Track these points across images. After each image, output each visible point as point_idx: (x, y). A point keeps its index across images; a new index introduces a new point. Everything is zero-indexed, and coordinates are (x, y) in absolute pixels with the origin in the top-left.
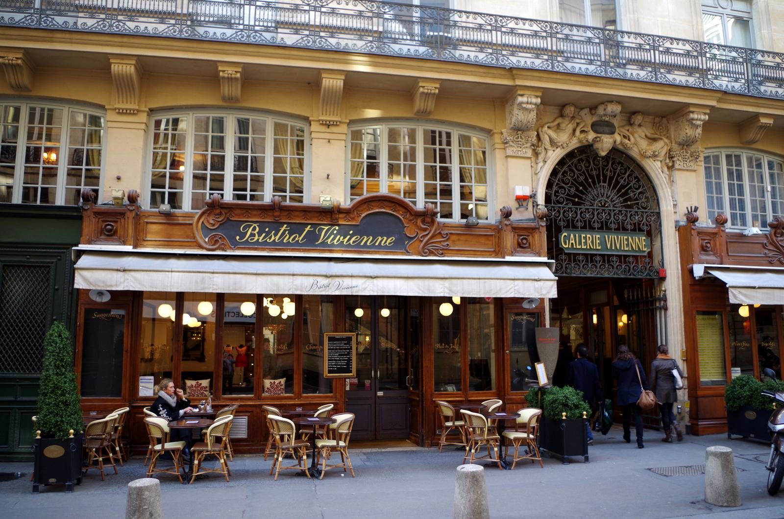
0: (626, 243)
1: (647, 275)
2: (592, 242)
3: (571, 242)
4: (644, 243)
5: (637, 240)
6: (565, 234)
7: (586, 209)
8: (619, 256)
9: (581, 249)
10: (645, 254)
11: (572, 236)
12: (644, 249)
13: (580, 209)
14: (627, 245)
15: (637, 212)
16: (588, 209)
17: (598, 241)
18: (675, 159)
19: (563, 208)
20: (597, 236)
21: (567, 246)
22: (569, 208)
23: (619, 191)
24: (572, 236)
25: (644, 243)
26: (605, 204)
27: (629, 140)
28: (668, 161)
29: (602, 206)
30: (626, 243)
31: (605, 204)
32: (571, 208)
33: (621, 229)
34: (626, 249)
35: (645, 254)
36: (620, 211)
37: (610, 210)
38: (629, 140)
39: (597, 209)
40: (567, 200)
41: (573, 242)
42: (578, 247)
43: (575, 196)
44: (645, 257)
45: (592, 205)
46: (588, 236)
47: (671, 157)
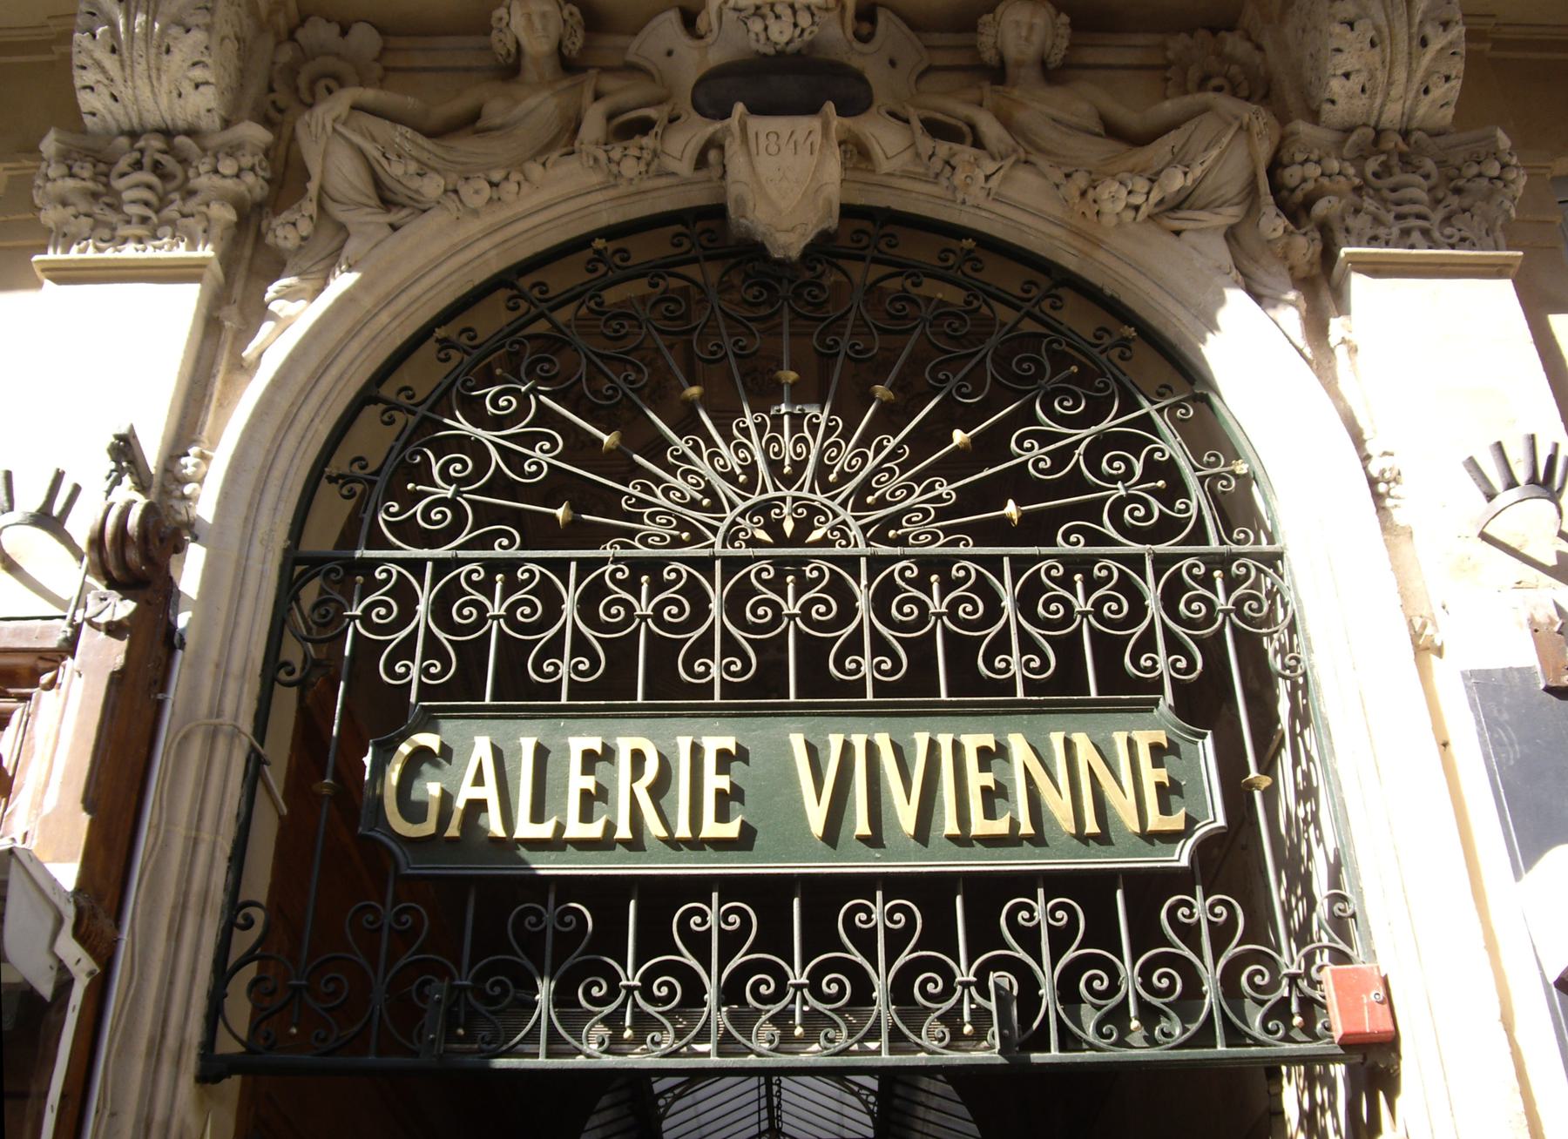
0: (977, 780)
1: (1205, 1037)
2: (660, 789)
4: (1151, 776)
6: (430, 740)
7: (638, 566)
8: (931, 892)
10: (1181, 856)
12: (1156, 821)
13: (586, 566)
17: (714, 782)
18: (1321, 208)
19: (442, 566)
20: (712, 745)
22: (492, 566)
23: (923, 441)
24: (482, 749)
25: (1151, 776)
26: (804, 527)
27: (978, 143)
28: (1273, 224)
29: (779, 539)
31: (804, 527)
32: (511, 566)
33: (946, 676)
34: (980, 825)
35: (1181, 856)
36: (928, 565)
37: (851, 563)
38: (978, 143)
39: (732, 565)
40: (485, 514)
41: (489, 792)
43: (555, 487)
45: (698, 537)
46: (625, 746)
47: (1296, 210)
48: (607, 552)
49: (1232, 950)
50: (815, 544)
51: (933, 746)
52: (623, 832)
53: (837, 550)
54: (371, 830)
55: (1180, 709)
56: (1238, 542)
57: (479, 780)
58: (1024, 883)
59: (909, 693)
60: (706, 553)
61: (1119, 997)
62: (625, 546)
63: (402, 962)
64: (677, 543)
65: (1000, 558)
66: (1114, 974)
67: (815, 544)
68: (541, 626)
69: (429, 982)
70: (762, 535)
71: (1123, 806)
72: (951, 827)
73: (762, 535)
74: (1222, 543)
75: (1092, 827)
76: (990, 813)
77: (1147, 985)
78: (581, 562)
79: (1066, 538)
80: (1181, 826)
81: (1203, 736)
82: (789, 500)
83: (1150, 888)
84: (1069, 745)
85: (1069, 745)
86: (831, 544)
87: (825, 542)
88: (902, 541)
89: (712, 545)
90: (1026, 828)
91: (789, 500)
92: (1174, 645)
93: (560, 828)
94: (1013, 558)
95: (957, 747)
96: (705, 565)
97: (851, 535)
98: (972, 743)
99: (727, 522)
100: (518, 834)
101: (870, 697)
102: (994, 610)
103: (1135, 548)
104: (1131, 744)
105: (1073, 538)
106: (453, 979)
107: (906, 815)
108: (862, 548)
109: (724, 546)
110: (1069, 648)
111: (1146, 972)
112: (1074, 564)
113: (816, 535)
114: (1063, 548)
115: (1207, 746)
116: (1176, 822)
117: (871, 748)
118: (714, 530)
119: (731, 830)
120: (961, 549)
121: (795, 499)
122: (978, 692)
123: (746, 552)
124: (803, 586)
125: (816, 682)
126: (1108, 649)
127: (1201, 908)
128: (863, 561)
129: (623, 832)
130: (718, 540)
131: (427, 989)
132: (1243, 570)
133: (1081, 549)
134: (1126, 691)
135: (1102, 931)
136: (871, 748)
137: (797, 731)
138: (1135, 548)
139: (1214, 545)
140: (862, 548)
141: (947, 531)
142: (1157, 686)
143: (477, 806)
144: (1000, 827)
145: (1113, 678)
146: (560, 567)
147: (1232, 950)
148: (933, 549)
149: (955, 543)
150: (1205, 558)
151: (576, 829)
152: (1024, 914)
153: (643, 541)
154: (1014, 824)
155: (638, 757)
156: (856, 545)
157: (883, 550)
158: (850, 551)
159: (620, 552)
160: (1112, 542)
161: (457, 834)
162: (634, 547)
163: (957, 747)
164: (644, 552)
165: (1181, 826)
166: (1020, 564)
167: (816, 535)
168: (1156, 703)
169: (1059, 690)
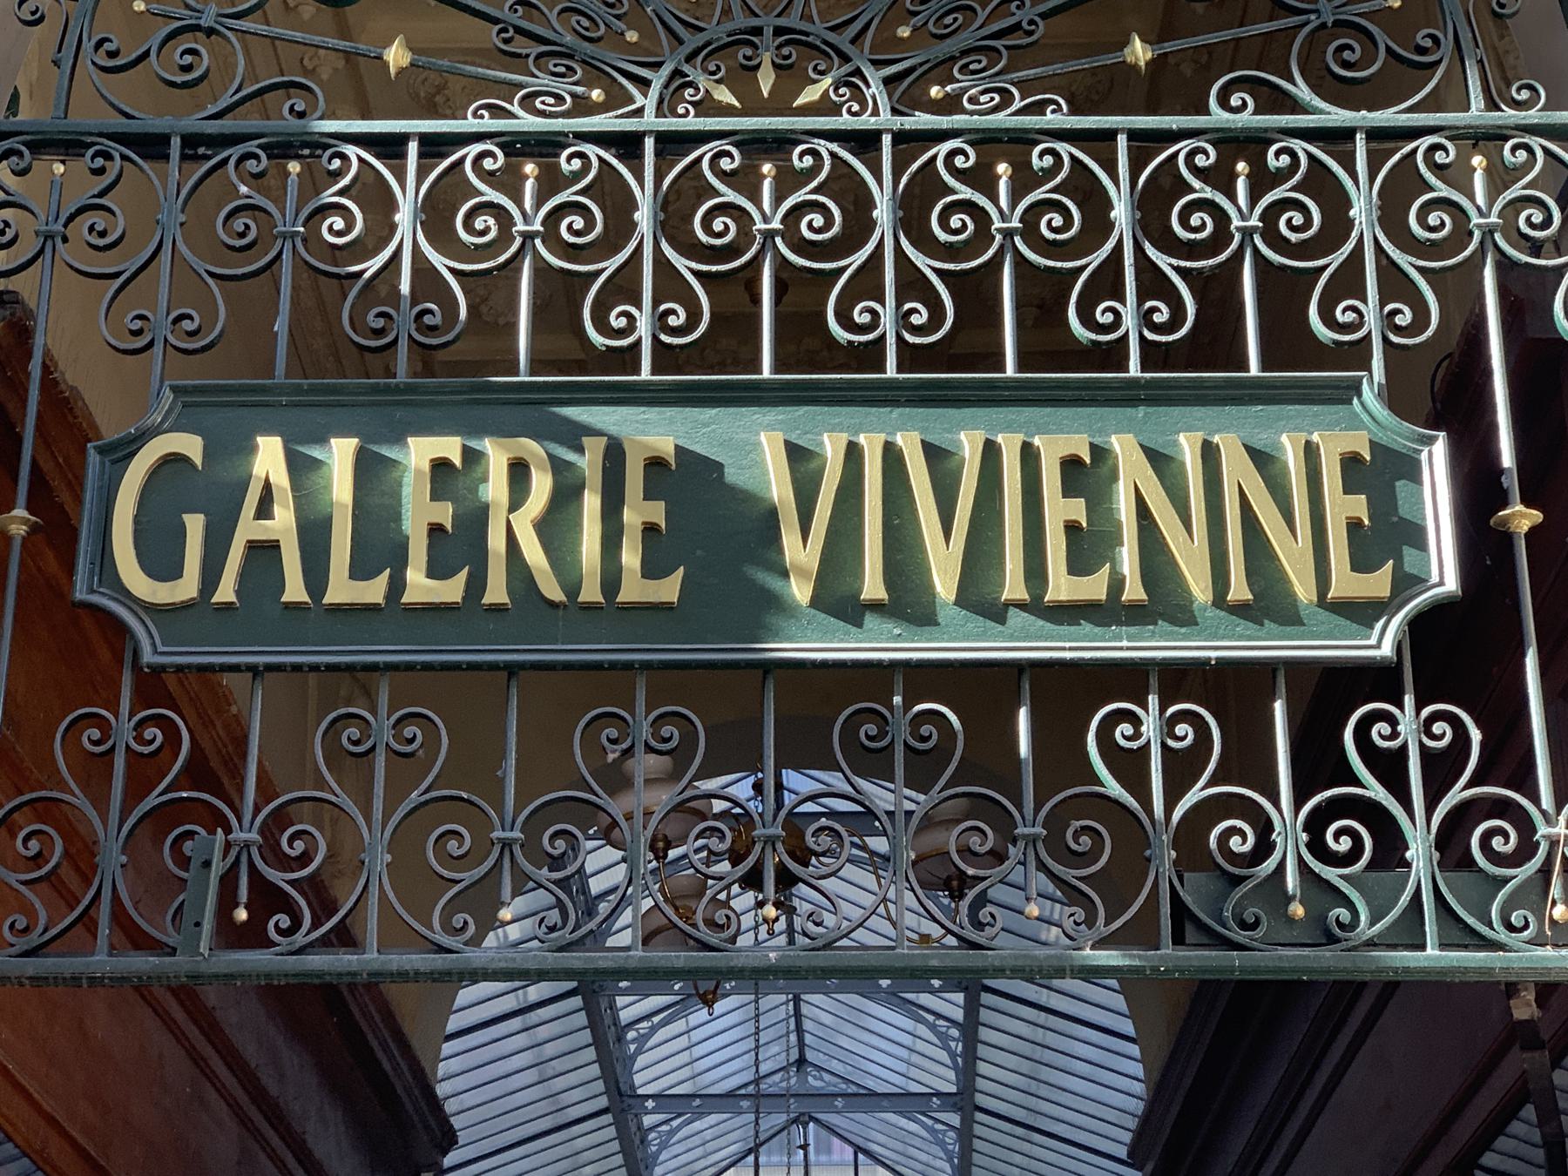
0: (1059, 509)
3: (248, 529)
4: (1343, 507)
5: (1237, 470)
7: (518, 146)
9: (395, 612)
10: (1383, 642)
11: (269, 458)
12: (1346, 582)
13: (434, 146)
14: (1087, 547)
15: (1251, 144)
16: (544, 146)
21: (186, 588)
24: (269, 458)
30: (1059, 509)
34: (1061, 586)
35: (1383, 642)
37: (865, 142)
39: (672, 144)
42: (342, 589)
44: (1377, 680)
48: (469, 124)
49: (1456, 795)
50: (806, 110)
51: (991, 451)
52: (497, 592)
53: (845, 121)
54: (92, 591)
55: (1394, 397)
56: (1517, 105)
57: (264, 511)
58: (1128, 679)
59: (952, 366)
60: (630, 125)
61: (1270, 864)
62: (497, 112)
63: (152, 800)
64: (583, 107)
65: (1111, 135)
66: (1264, 828)
67: (806, 110)
68: (361, 250)
69: (190, 835)
70: (724, 95)
71: (1293, 555)
72: (1014, 586)
73: (724, 95)
74: (1492, 105)
75: (1239, 590)
76: (1078, 565)
77: (1318, 847)
78: (426, 140)
79: (1224, 103)
80: (1385, 592)
81: (1430, 441)
82: (768, 32)
83: (1331, 691)
84: (1209, 454)
85: (1209, 454)
86: (835, 110)
87: (826, 107)
88: (950, 105)
89: (639, 112)
90: (1134, 591)
91: (768, 32)
92: (1394, 284)
93: (397, 586)
94: (1133, 135)
95: (1029, 455)
96: (627, 145)
97: (868, 94)
98: (1052, 449)
99: (666, 71)
100: (330, 598)
101: (891, 371)
102: (1098, 223)
103: (1338, 116)
104: (1311, 451)
105: (1235, 101)
106: (228, 831)
107: (944, 572)
108: (885, 119)
109: (660, 113)
110: (1217, 292)
111: (1316, 825)
112: (1234, 144)
113: (810, 95)
114: (1218, 116)
115: (1436, 458)
116: (1378, 584)
117: (892, 458)
118: (644, 84)
119: (669, 589)
120: (1051, 119)
121: (778, 31)
122: (1067, 367)
123: (693, 123)
124: (788, 181)
125: (803, 340)
126: (1283, 293)
127: (1408, 726)
128: (887, 140)
129: (497, 592)
130: (649, 102)
131: (188, 846)
132: (1522, 155)
133: (1248, 119)
134: (1307, 365)
135: (1249, 760)
136: (892, 458)
137: (770, 427)
138: (1338, 116)
139: (1476, 112)
140: (885, 119)
141: (1026, 87)
142: (1358, 354)
143: (264, 552)
144: (1094, 588)
145: (1288, 340)
146: (390, 147)
147: (1456, 795)
148: (1002, 119)
149: (1038, 108)
150: (1456, 134)
151: (420, 585)
152: (1126, 728)
153: (527, 102)
154: (1117, 584)
155: (519, 471)
156: (876, 113)
157: (922, 120)
158: (867, 122)
159: (489, 124)
160: (1296, 107)
161: (232, 598)
162: (513, 116)
163: (1029, 455)
164: (528, 122)
165: (1385, 592)
166: (1145, 143)
167: (810, 95)
168: (1356, 388)
169: (1199, 358)
